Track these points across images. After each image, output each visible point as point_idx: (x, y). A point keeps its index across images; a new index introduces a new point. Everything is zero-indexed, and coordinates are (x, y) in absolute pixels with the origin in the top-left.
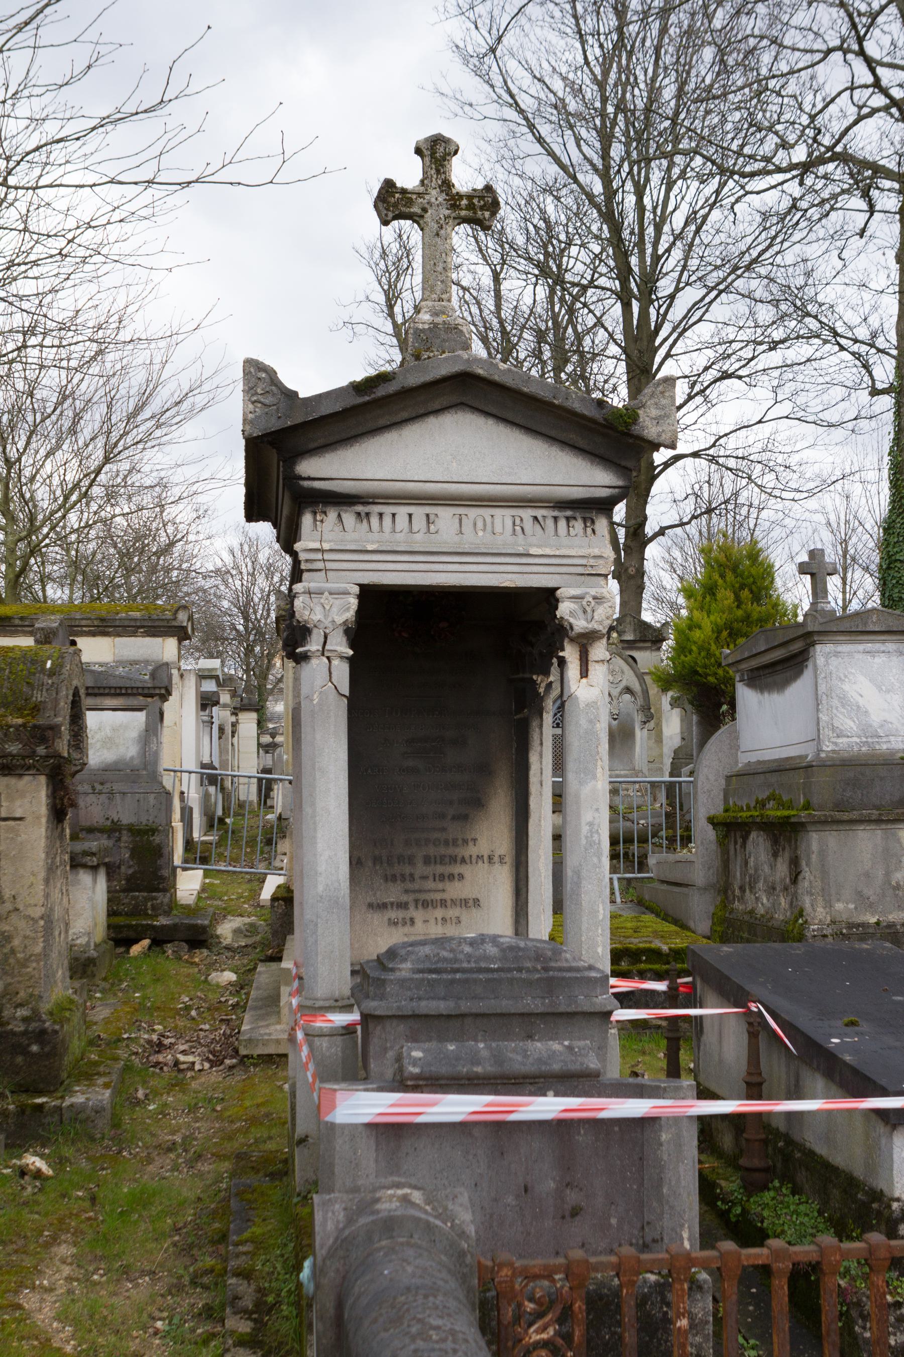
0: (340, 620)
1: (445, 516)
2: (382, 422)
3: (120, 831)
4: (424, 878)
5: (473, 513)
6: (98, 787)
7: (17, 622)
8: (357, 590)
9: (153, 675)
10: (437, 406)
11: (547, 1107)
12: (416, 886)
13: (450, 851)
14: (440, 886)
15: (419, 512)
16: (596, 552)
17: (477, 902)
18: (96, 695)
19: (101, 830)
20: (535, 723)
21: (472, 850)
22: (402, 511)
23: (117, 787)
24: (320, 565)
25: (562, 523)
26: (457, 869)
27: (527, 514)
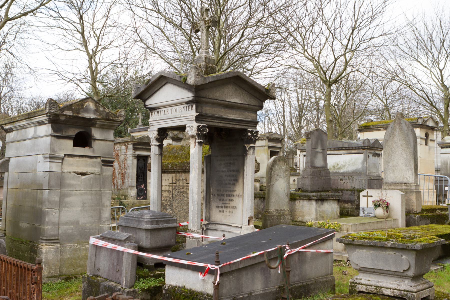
0: (154, 137)
1: (169, 109)
2: (156, 90)
3: (354, 190)
4: (226, 200)
5: (173, 108)
6: (350, 177)
7: (372, 127)
8: (157, 129)
9: (364, 143)
10: (163, 84)
11: (110, 246)
12: (224, 202)
13: (231, 193)
14: (229, 202)
15: (166, 109)
16: (192, 114)
17: (236, 207)
18: (350, 149)
19: (350, 190)
20: (246, 158)
21: (235, 193)
22: (163, 109)
23: (355, 177)
24: (152, 125)
25: (188, 108)
26: (232, 198)
27: (182, 106)
